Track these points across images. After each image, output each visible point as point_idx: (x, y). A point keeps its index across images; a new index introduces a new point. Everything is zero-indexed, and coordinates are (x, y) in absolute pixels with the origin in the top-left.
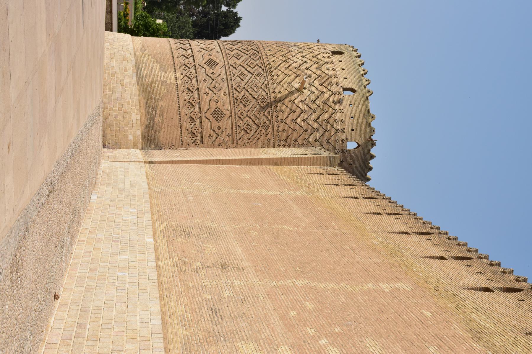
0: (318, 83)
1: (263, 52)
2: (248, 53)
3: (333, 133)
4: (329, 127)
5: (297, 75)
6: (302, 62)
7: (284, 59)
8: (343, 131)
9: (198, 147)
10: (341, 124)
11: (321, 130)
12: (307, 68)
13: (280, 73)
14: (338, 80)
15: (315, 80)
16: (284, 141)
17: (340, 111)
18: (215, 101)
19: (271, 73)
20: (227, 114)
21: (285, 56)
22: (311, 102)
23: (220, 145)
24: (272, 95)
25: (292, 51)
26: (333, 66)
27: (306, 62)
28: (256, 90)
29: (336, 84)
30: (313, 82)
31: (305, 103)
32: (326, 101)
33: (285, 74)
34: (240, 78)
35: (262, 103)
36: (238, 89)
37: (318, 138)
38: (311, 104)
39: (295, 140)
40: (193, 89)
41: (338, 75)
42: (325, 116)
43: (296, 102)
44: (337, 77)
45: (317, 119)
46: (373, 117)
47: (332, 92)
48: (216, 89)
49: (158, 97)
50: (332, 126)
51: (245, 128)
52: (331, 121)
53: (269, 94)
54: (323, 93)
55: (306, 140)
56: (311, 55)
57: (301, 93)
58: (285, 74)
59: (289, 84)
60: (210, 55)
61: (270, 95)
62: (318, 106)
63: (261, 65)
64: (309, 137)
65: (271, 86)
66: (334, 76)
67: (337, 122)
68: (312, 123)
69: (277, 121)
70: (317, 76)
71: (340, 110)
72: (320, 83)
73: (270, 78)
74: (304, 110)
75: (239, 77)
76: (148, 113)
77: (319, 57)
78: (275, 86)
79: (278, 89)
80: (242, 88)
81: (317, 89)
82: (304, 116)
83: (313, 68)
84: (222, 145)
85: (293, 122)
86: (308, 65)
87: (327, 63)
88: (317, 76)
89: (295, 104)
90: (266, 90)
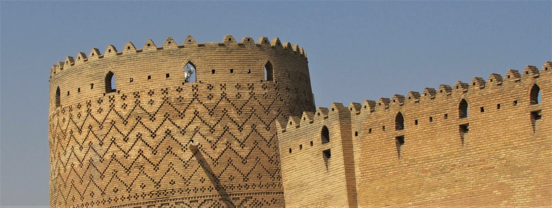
0: (181, 120)
4: (247, 109)
7: (135, 171)
10: (242, 89)
12: (151, 136)
13: (166, 180)
14: (172, 89)
15: (174, 124)
16: (273, 177)
19: (167, 193)
22: (212, 132)
24: (207, 193)
26: (143, 93)
29: (180, 92)
30: (179, 127)
31: (215, 143)
32: (209, 110)
33: (168, 171)
38: (217, 134)
39: (271, 160)
41: (162, 88)
42: (233, 113)
43: (216, 156)
44: (167, 89)
45: (238, 126)
46: (230, 39)
47: (193, 99)
50: (246, 103)
52: (239, 104)
53: (205, 198)
54: (196, 113)
55: (269, 145)
57: (200, 148)
58: (168, 171)
59: (186, 165)
61: (207, 196)
62: (217, 123)
65: (192, 194)
66: (165, 94)
70: (167, 121)
71: (221, 88)
72: (180, 116)
73: (177, 195)
74: (226, 145)
77: (124, 113)
78: (191, 187)
79: (195, 183)
81: (190, 123)
82: (235, 145)
83: (153, 126)
85: (246, 163)
86: (146, 135)
87: (137, 103)
88: (167, 121)
89: (219, 158)
90: (200, 202)
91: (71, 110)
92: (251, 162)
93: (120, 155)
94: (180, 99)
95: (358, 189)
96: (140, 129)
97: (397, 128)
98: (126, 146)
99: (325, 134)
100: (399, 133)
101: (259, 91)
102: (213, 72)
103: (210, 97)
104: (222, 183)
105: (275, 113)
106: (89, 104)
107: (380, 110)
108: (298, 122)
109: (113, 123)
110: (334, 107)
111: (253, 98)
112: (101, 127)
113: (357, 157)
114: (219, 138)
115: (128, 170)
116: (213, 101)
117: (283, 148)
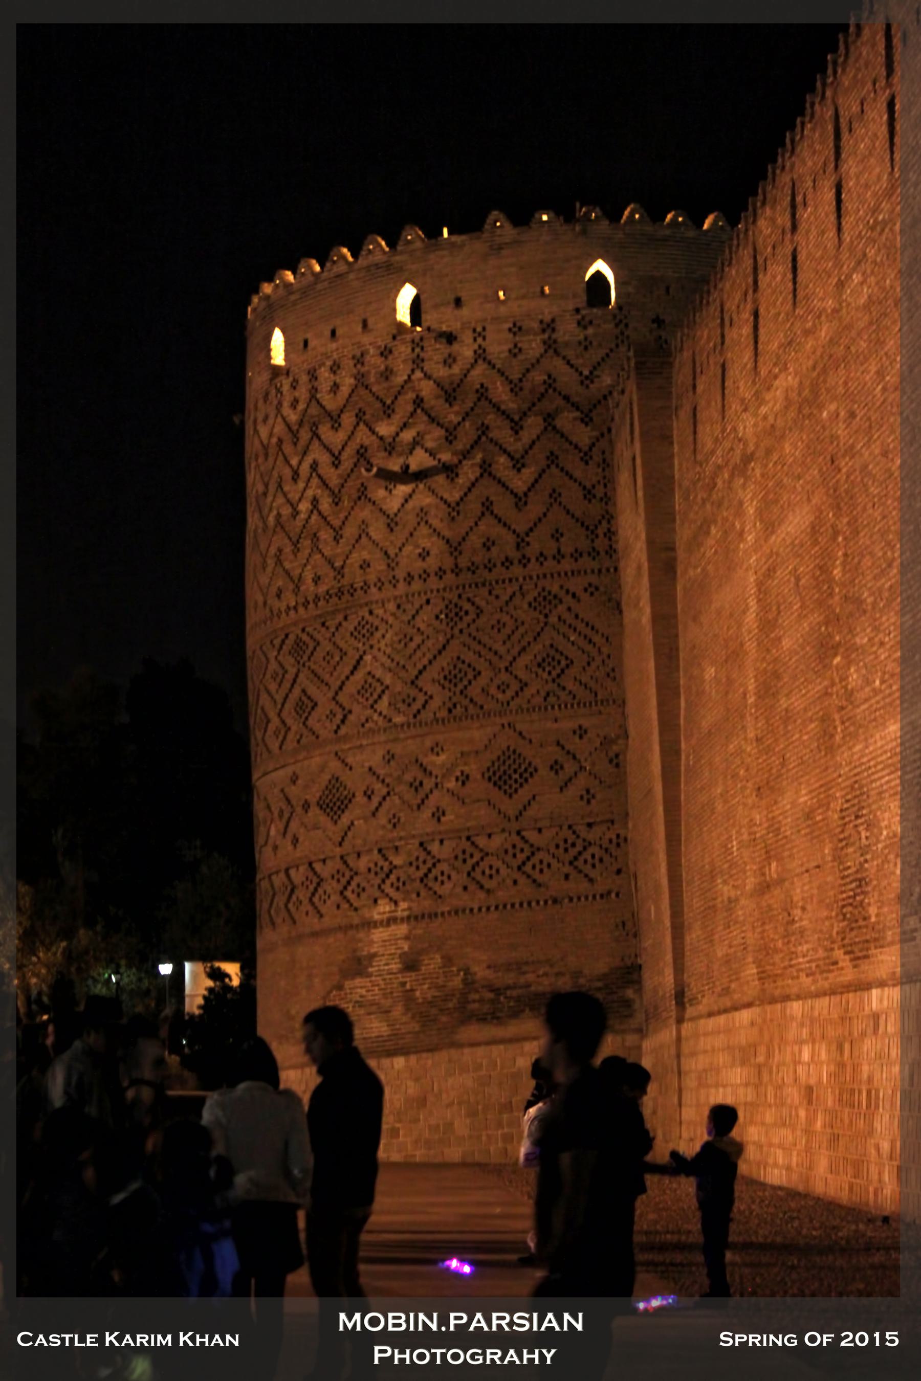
1: (284, 620)
2: (292, 671)
3: (559, 363)
5: (359, 498)
6: (315, 481)
8: (548, 326)
9: (626, 840)
13: (356, 558)
14: (372, 351)
17: (479, 340)
18: (463, 783)
21: (294, 539)
22: (451, 442)
23: (616, 761)
25: (279, 515)
27: (314, 466)
28: (418, 640)
34: (380, 697)
35: (461, 619)
36: (418, 705)
37: (577, 414)
38: (461, 445)
39: (588, 494)
40: (424, 862)
42: (500, 391)
43: (454, 496)
44: (362, 355)
45: (512, 420)
48: (421, 784)
49: (457, 982)
51: (554, 674)
54: (419, 402)
55: (586, 458)
56: (288, 448)
60: (306, 806)
64: (576, 447)
67: (520, 350)
68: (527, 436)
69: (524, 561)
75: (376, 702)
76: (515, 1014)
77: (293, 417)
78: (400, 574)
80: (413, 692)
84: (617, 756)
94: (387, 374)
102: (458, 302)
111: (551, 352)
116: (456, 370)
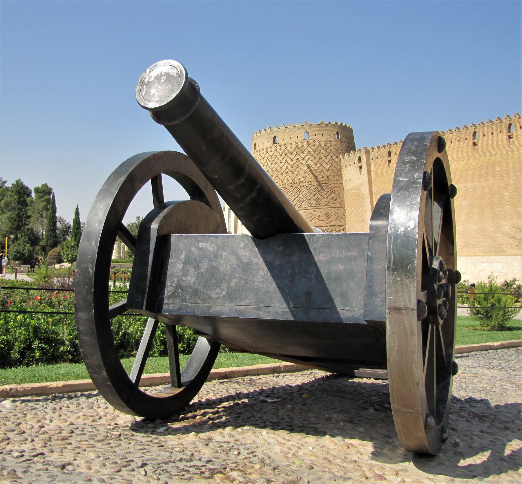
4: (329, 150)
7: (285, 175)
11: (331, 154)
20: (326, 210)
24: (313, 183)
28: (310, 193)
38: (317, 160)
39: (338, 170)
42: (323, 152)
43: (316, 169)
52: (326, 148)
54: (309, 152)
63: (292, 189)
73: (301, 184)
77: (281, 152)
79: (308, 179)
82: (324, 164)
83: (292, 157)
87: (286, 148)
91: (260, 151)
92: (330, 171)
93: (279, 168)
94: (302, 146)
95: (372, 181)
96: (286, 158)
97: (388, 157)
98: (281, 165)
99: (360, 159)
100: (389, 159)
101: (333, 143)
102: (316, 135)
103: (314, 145)
104: (319, 179)
105: (340, 152)
106: (267, 149)
107: (382, 150)
108: (349, 155)
109: (276, 156)
110: (363, 148)
112: (272, 158)
113: (372, 168)
114: (318, 162)
115: (282, 174)
117: (343, 166)
